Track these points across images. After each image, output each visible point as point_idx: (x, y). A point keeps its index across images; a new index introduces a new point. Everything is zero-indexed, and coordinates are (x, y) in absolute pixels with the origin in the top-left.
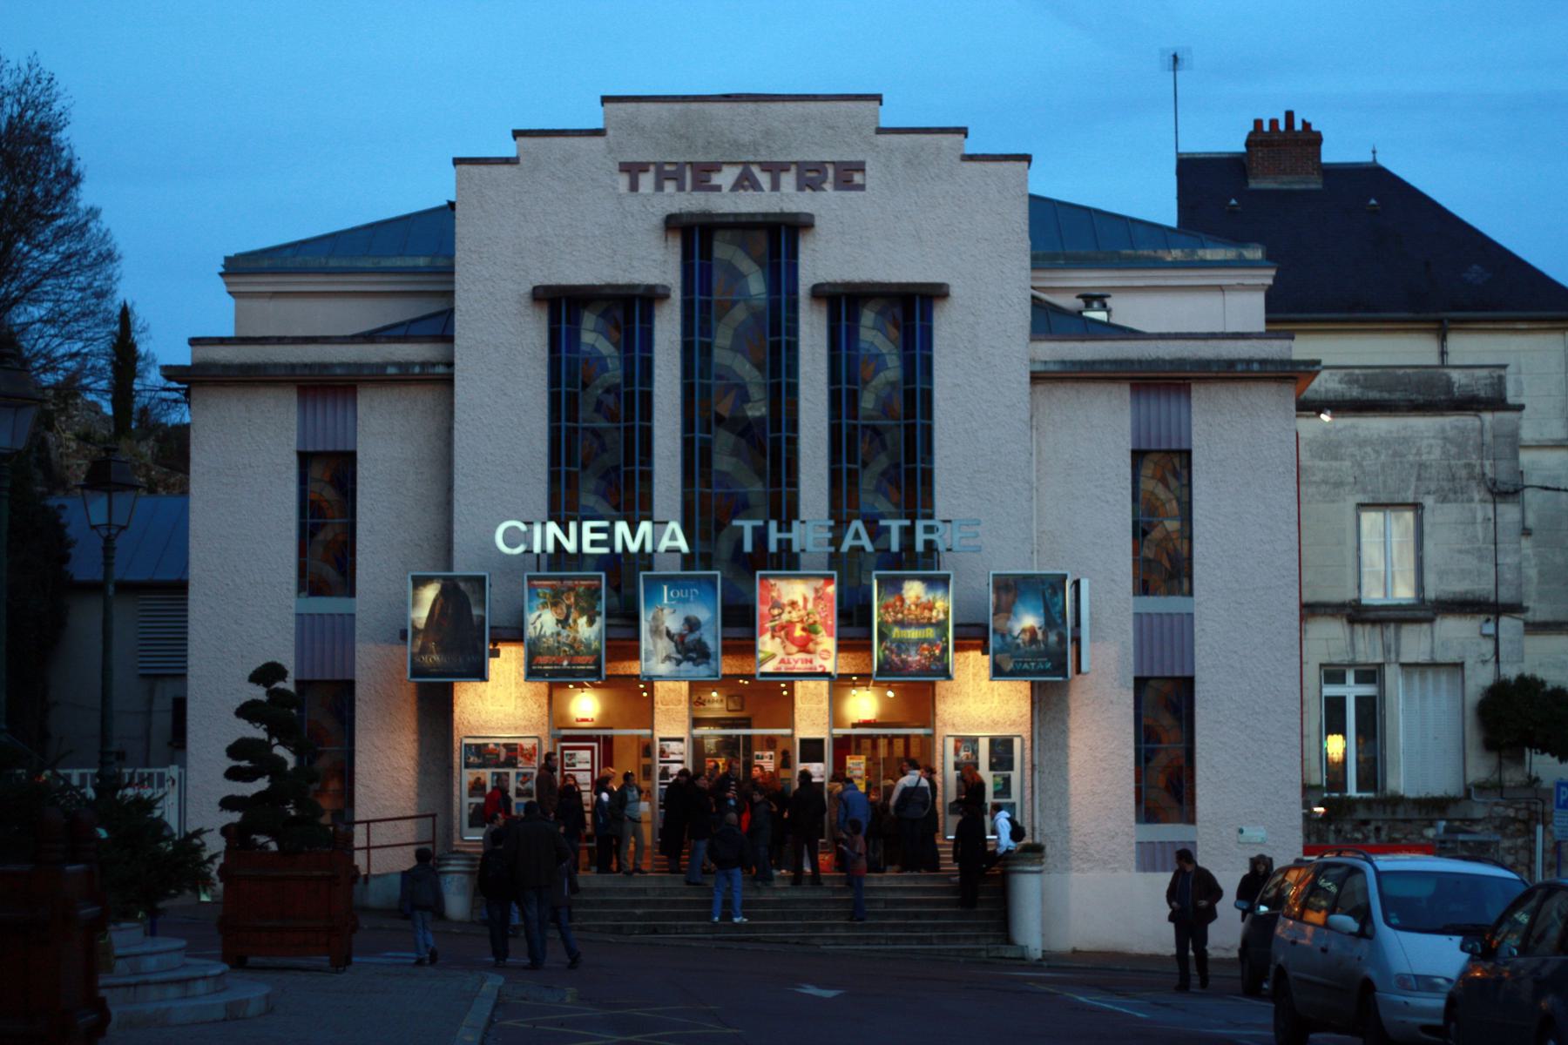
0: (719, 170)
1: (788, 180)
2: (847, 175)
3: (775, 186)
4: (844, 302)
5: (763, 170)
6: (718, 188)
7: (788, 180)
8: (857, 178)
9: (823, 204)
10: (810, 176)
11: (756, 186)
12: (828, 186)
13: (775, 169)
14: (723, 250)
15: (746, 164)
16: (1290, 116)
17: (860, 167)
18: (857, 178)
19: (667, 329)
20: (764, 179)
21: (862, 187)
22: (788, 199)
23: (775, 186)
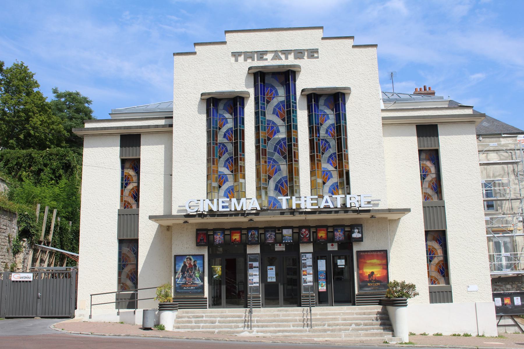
0: (266, 54)
1: (291, 57)
2: (313, 53)
3: (287, 58)
4: (313, 97)
5: (282, 54)
6: (266, 59)
7: (291, 57)
8: (316, 55)
9: (304, 63)
10: (299, 54)
11: (281, 59)
12: (305, 57)
13: (286, 53)
14: (268, 80)
15: (275, 51)
16: (425, 87)
17: (316, 51)
18: (316, 55)
19: (249, 109)
20: (283, 57)
21: (318, 57)
22: (291, 61)
23: (287, 58)
